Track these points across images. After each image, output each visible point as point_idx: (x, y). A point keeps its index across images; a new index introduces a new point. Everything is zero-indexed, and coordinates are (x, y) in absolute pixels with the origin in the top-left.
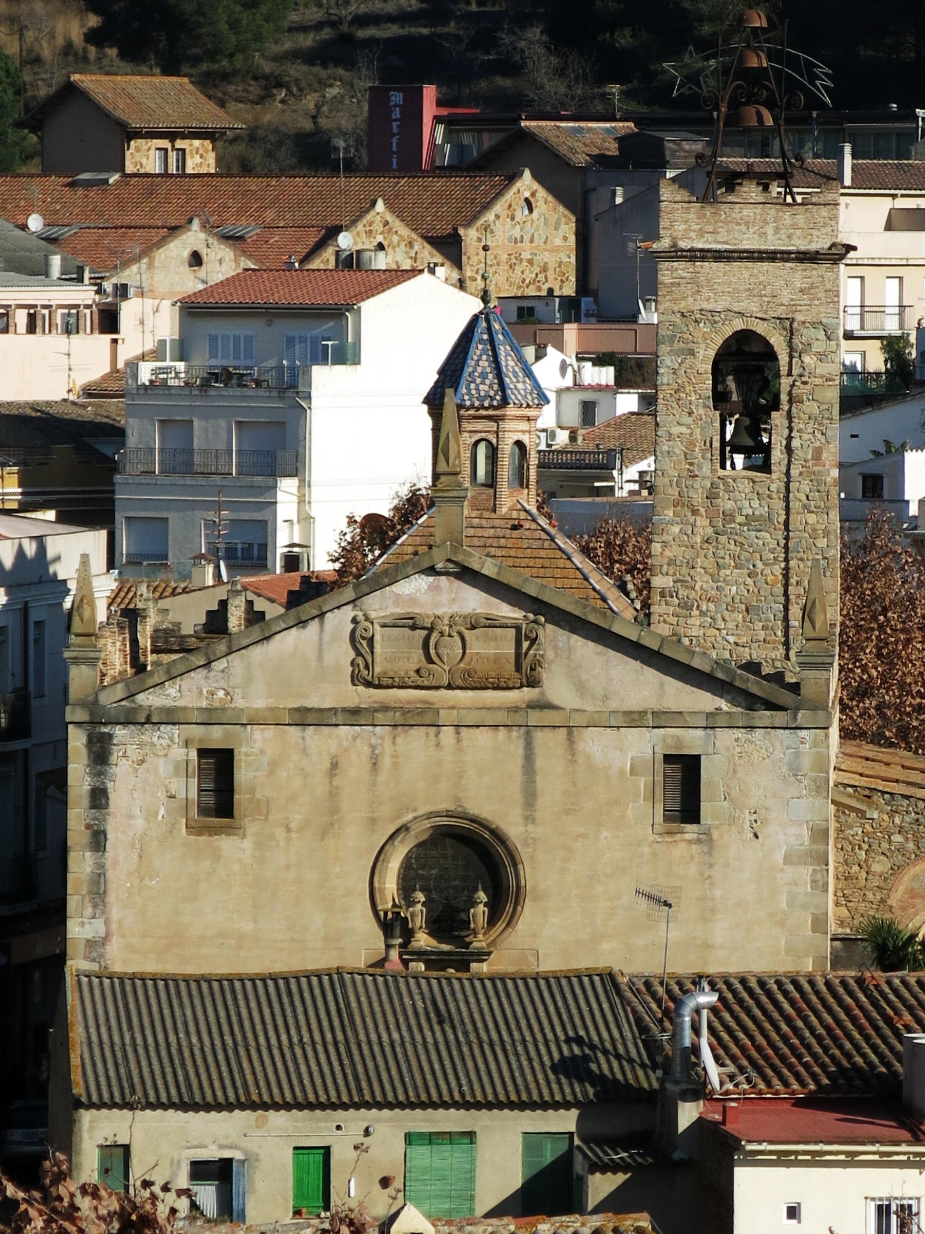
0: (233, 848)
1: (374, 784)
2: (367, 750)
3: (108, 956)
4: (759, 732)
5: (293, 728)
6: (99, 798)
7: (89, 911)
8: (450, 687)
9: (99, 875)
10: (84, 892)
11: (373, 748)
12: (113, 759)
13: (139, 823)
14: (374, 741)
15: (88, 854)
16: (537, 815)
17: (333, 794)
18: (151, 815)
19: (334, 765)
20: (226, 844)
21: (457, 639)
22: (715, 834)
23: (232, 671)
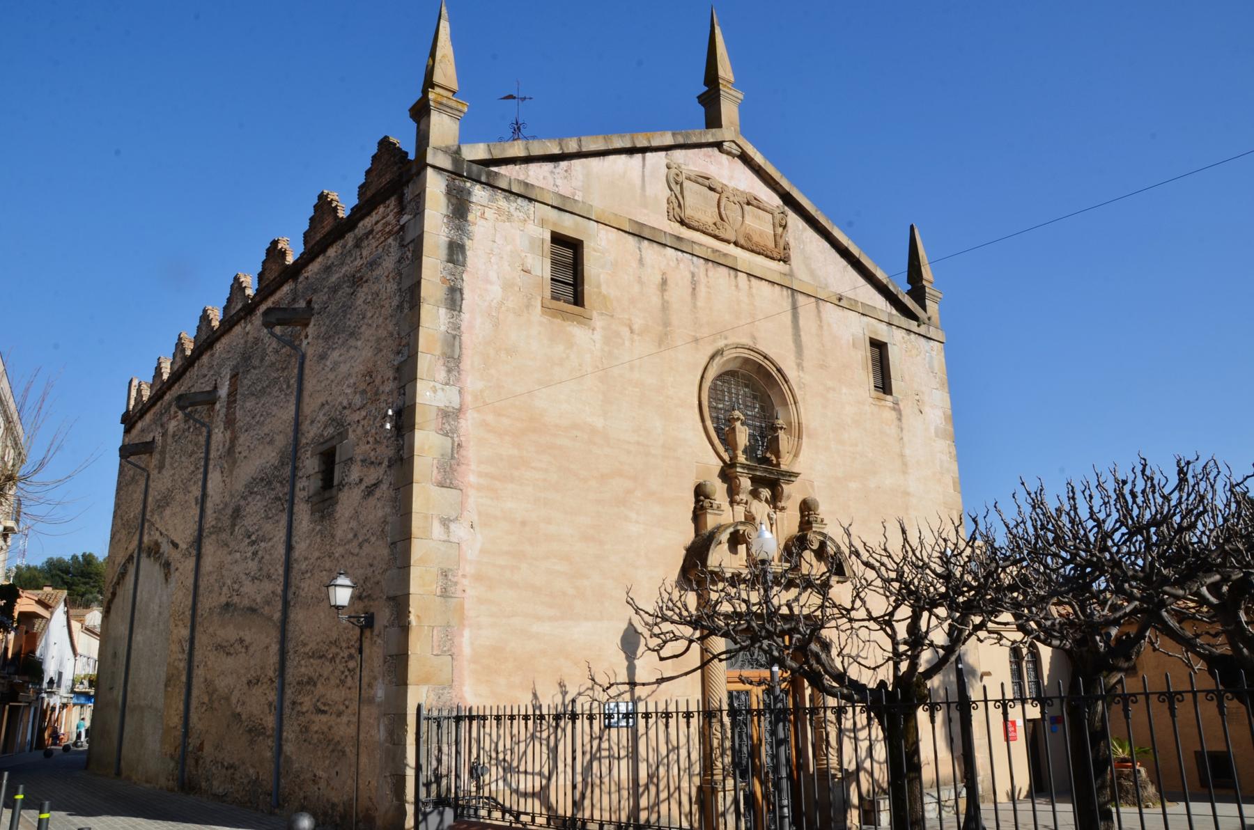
0: (585, 338)
1: (695, 306)
2: (689, 276)
3: (462, 431)
4: (913, 336)
5: (630, 238)
6: (456, 251)
7: (441, 374)
8: (736, 244)
9: (454, 337)
10: (438, 352)
11: (693, 275)
12: (471, 217)
13: (496, 291)
14: (692, 268)
15: (443, 311)
16: (805, 364)
17: (665, 307)
18: (507, 286)
19: (664, 282)
20: (578, 332)
21: (738, 206)
22: (902, 405)
23: (573, 173)
